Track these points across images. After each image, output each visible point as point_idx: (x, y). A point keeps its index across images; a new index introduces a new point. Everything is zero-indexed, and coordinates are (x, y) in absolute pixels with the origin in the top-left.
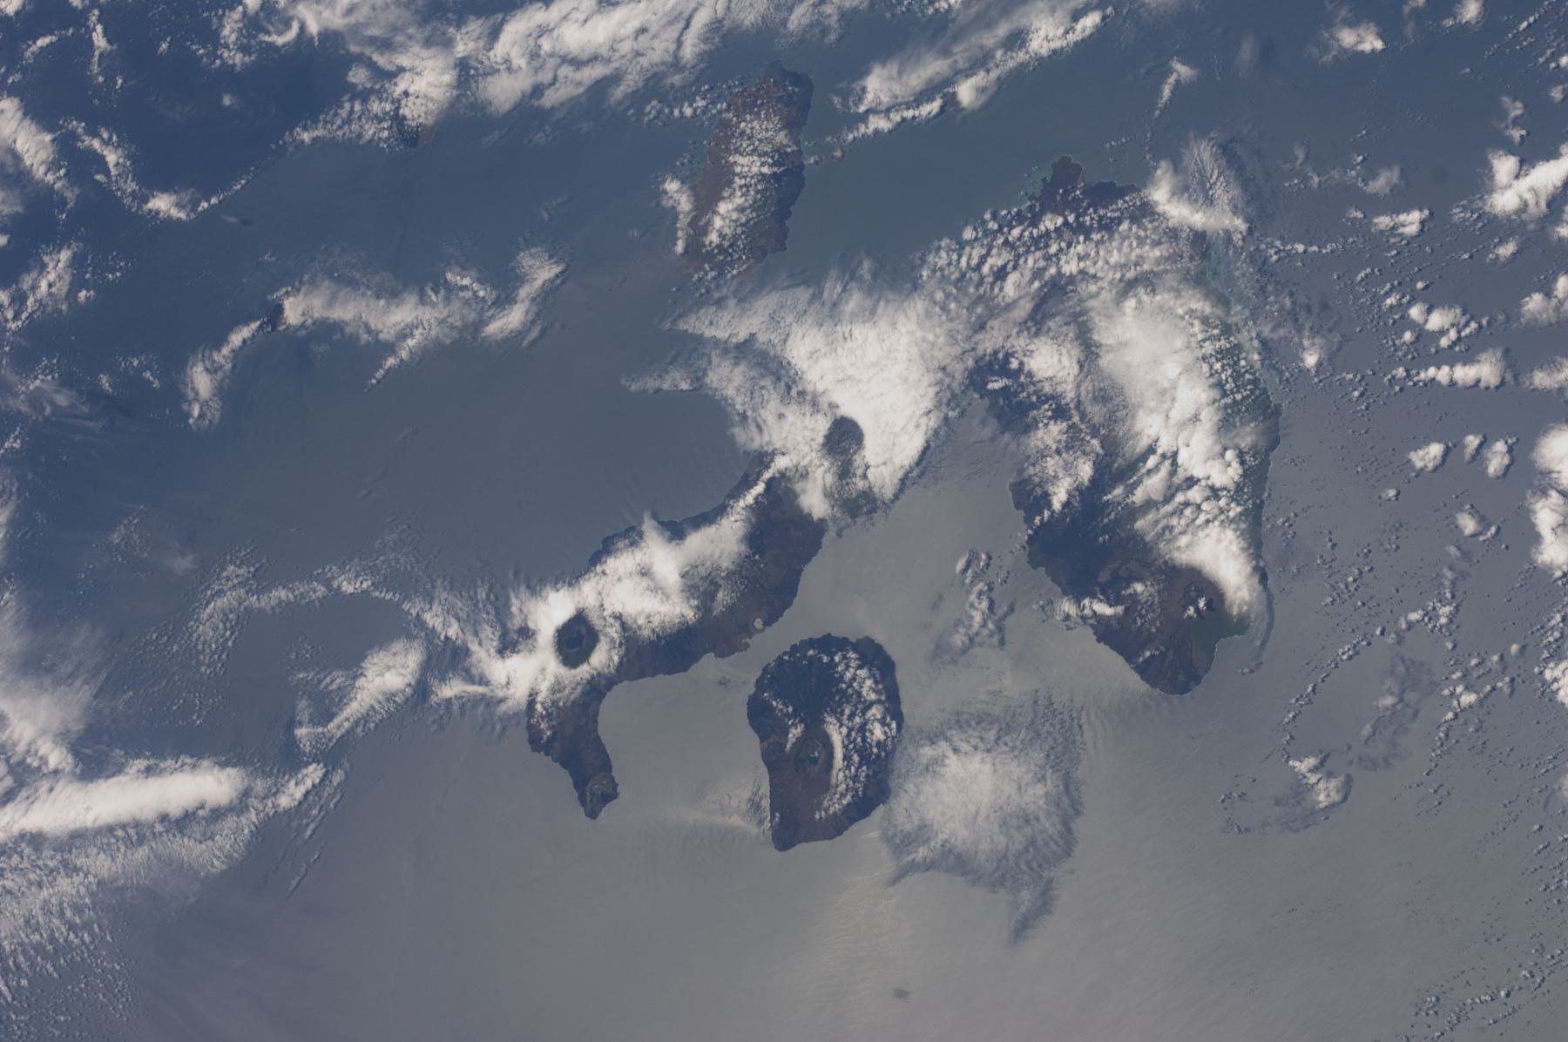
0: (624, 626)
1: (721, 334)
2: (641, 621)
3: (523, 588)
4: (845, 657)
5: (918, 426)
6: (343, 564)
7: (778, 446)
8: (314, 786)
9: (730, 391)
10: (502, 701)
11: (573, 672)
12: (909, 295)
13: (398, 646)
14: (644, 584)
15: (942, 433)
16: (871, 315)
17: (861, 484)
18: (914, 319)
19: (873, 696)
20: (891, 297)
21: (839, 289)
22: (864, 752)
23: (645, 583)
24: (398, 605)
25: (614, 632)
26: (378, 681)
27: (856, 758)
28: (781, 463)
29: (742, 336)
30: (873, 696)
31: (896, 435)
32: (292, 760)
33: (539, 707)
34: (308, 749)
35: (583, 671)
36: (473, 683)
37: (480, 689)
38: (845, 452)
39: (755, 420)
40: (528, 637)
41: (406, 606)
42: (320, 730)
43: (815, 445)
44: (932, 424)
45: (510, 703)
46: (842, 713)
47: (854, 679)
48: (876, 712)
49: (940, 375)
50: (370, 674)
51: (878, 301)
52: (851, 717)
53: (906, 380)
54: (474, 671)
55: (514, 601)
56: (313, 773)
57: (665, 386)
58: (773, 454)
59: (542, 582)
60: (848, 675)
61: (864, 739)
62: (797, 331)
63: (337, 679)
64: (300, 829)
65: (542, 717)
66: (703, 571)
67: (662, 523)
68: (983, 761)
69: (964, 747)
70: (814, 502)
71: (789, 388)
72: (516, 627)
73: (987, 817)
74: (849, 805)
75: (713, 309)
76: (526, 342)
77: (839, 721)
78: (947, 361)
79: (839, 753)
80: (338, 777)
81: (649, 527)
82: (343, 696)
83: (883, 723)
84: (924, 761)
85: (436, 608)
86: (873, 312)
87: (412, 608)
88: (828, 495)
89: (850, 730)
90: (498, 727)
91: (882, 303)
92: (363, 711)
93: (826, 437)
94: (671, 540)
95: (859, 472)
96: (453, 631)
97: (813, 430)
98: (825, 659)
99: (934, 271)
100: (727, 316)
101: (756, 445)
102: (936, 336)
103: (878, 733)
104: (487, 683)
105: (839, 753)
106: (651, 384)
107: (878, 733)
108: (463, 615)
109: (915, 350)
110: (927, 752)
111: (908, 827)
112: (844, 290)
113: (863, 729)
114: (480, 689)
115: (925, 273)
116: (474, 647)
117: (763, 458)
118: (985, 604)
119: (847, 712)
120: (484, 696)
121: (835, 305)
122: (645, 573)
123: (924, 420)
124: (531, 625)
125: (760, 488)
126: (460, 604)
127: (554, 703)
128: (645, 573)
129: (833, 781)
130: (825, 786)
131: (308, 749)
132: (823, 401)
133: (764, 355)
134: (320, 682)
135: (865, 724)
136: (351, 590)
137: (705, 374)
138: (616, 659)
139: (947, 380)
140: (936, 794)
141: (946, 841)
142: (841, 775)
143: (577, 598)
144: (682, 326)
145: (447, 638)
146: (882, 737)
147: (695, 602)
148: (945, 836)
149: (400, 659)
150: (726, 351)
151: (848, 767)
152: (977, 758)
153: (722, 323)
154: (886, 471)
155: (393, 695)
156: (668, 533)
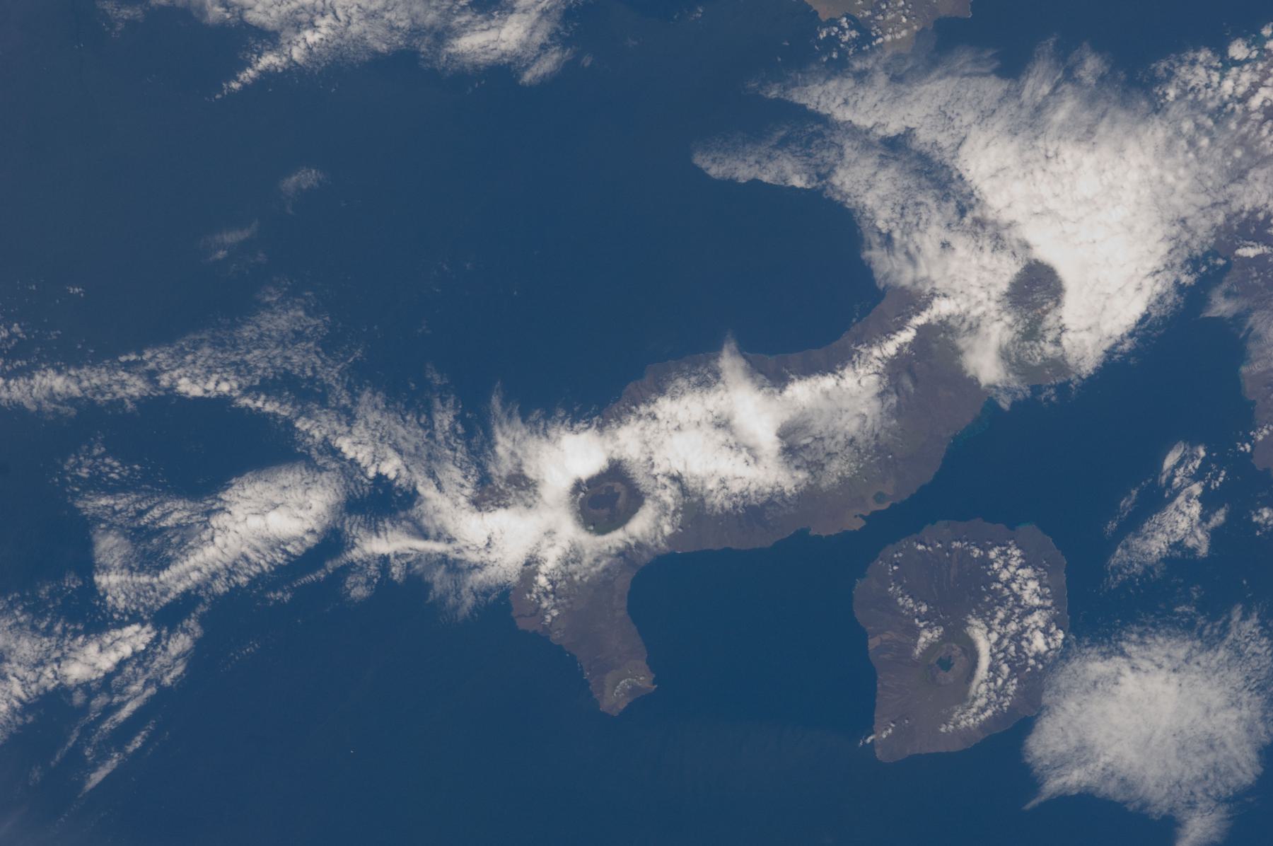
0: (684, 491)
1: (862, 119)
2: (711, 485)
3: (518, 422)
4: (1004, 553)
5: (1139, 289)
6: (182, 352)
7: (937, 286)
8: (135, 654)
9: (870, 200)
10: (479, 567)
11: (600, 539)
12: (1145, 118)
13: (291, 476)
14: (720, 437)
15: (1169, 301)
16: (1088, 135)
17: (1049, 349)
18: (1150, 150)
19: (1037, 601)
20: (1122, 115)
21: (1046, 89)
22: (1017, 665)
23: (721, 436)
24: (288, 423)
25: (669, 496)
26: (255, 522)
27: (1005, 668)
28: (942, 308)
29: (894, 127)
30: (1037, 601)
31: (1109, 296)
32: (93, 617)
33: (542, 580)
34: (121, 604)
35: (616, 538)
36: (426, 537)
37: (439, 547)
38: (1034, 306)
39: (905, 245)
40: (523, 489)
41: (302, 424)
42: (145, 579)
43: (994, 294)
44: (1158, 288)
45: (491, 572)
46: (993, 618)
47: (1013, 579)
48: (1037, 618)
49: (1178, 227)
50: (238, 511)
51: (1103, 116)
52: (1004, 623)
53: (1130, 229)
54: (425, 522)
55: (500, 438)
56: (134, 638)
57: (766, 178)
58: (933, 294)
59: (549, 415)
60: (1004, 575)
61: (1019, 649)
62: (977, 138)
63: (177, 512)
64: (110, 710)
65: (546, 594)
66: (830, 445)
67: (745, 357)
68: (1167, 681)
69: (1146, 665)
70: (985, 364)
71: (962, 212)
72: (504, 474)
73: (1163, 741)
74: (988, 719)
75: (850, 83)
76: (528, 77)
77: (988, 625)
78: (1191, 211)
79: (984, 661)
80: (180, 644)
81: (730, 363)
82: (185, 537)
83: (1046, 632)
84: (1093, 677)
85: (359, 429)
86: (1091, 131)
87: (314, 428)
88: (1004, 354)
89: (1002, 637)
90: (469, 601)
91: (1106, 120)
92: (228, 560)
93: (1012, 284)
94: (761, 387)
95: (1050, 336)
96: (391, 467)
97: (994, 271)
98: (977, 552)
99: (1185, 93)
100: (872, 98)
101: (906, 277)
102: (1179, 178)
103: (1039, 643)
104: (450, 540)
105: (984, 661)
106: (743, 171)
107: (1039, 643)
108: (404, 445)
109: (1145, 192)
110: (1098, 667)
111: (1062, 748)
112: (1053, 92)
113: (1018, 637)
114: (439, 547)
115: (1172, 93)
116: (427, 490)
117: (915, 300)
118: (1196, 509)
119: (1001, 615)
120: (444, 559)
121: (1038, 110)
122: (723, 424)
123: (1150, 281)
124: (530, 473)
125: (907, 336)
126: (401, 431)
127: (568, 576)
128: (723, 424)
129: (972, 692)
130: (961, 696)
131: (121, 604)
132: (1011, 236)
133: (923, 158)
134: (141, 513)
135: (1025, 629)
136: (196, 391)
137: (832, 171)
138: (668, 530)
139: (1186, 236)
140: (1103, 714)
141: (1109, 764)
142: (983, 687)
143: (609, 446)
144: (797, 97)
145: (380, 477)
146: (1045, 648)
147: (801, 475)
148: (1108, 759)
149: (295, 496)
150: (867, 146)
151: (994, 680)
152: (1162, 676)
153: (863, 106)
154: (1089, 340)
155: (283, 543)
156: (762, 377)
